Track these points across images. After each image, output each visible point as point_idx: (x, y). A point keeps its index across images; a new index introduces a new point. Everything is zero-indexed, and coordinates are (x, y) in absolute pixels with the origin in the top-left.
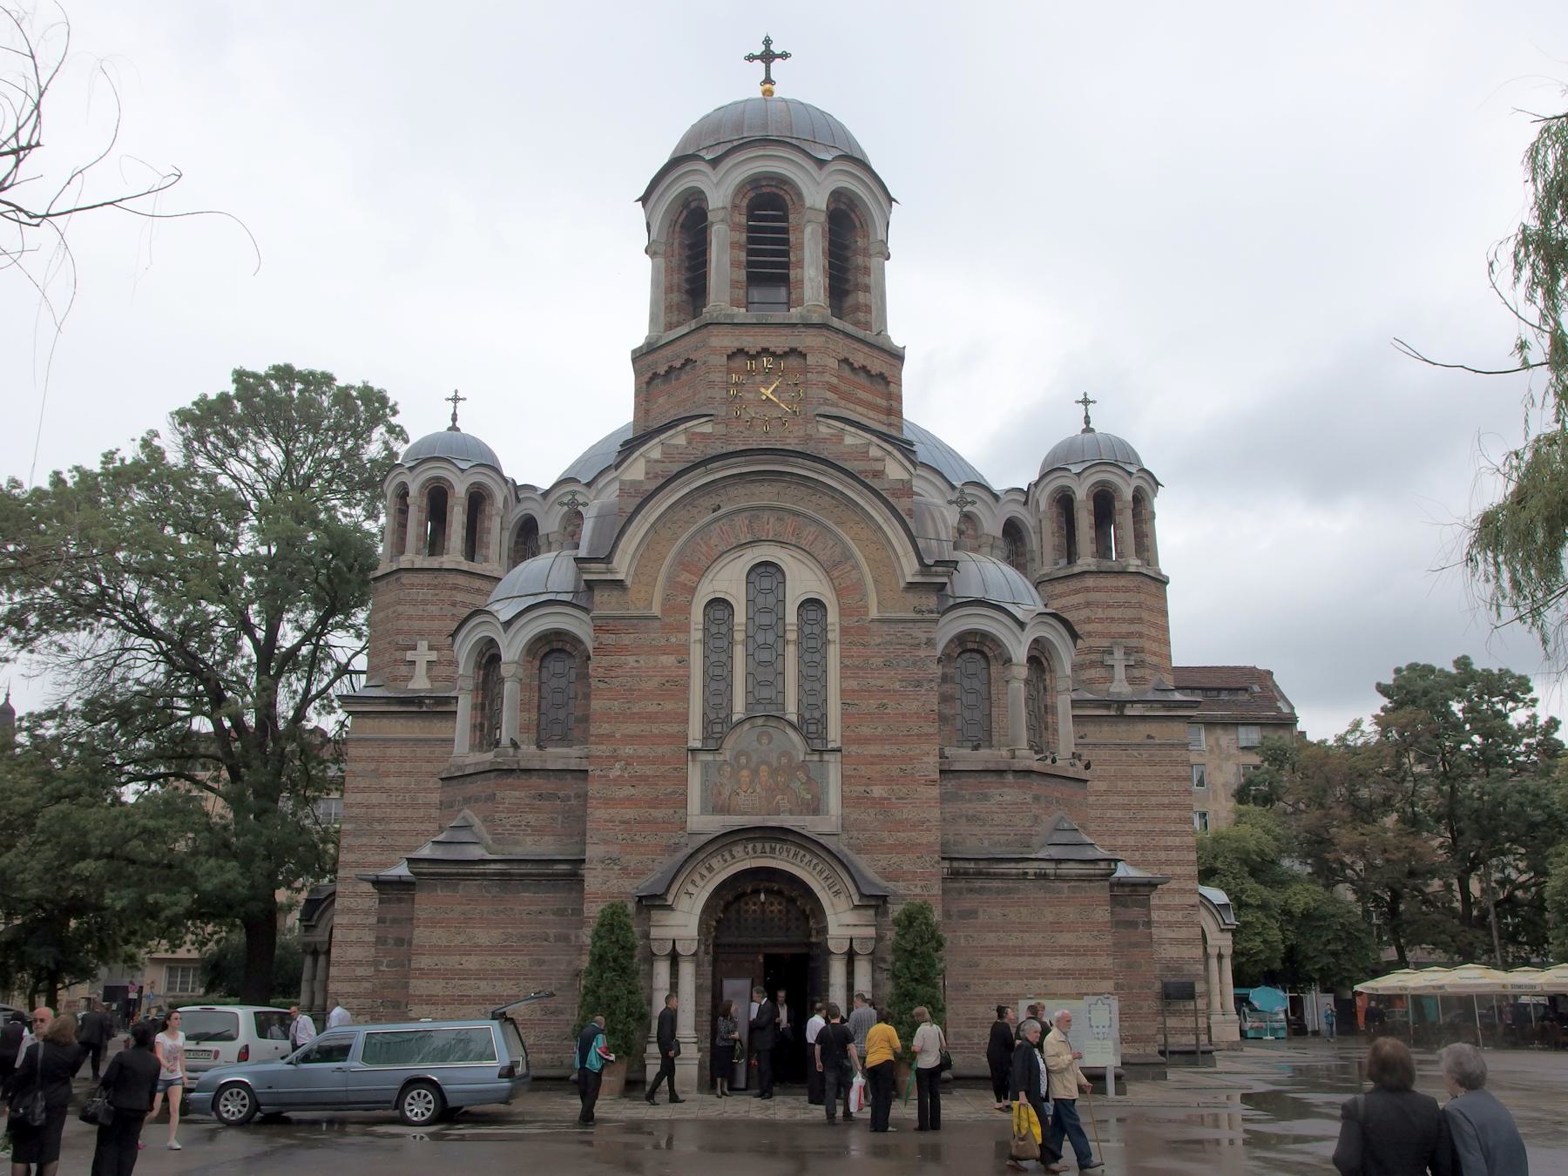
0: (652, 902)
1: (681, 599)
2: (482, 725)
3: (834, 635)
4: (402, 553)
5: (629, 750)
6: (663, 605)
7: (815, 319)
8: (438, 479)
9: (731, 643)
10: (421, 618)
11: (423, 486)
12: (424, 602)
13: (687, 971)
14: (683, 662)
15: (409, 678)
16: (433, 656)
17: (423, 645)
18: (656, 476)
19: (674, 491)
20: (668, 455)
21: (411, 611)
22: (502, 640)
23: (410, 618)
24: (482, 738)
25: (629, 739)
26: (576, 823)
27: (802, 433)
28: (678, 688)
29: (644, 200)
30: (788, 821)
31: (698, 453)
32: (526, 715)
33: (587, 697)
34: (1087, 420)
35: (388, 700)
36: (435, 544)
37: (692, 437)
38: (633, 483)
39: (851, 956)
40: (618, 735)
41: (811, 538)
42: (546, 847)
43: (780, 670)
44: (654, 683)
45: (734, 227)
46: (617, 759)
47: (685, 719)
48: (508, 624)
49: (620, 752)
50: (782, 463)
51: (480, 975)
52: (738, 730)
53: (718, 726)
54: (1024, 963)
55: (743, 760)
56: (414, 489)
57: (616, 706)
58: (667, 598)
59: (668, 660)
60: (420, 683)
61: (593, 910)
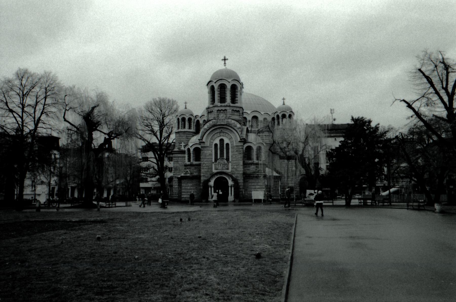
0: (209, 181)
3: (230, 147)
5: (205, 163)
7: (228, 105)
13: (213, 189)
17: (183, 143)
22: (190, 148)
25: (206, 161)
26: (200, 171)
28: (211, 155)
29: (207, 85)
30: (225, 171)
34: (284, 102)
39: (231, 187)
42: (195, 174)
45: (218, 91)
51: (190, 189)
53: (216, 159)
54: (254, 187)
59: (210, 151)
61: (202, 181)
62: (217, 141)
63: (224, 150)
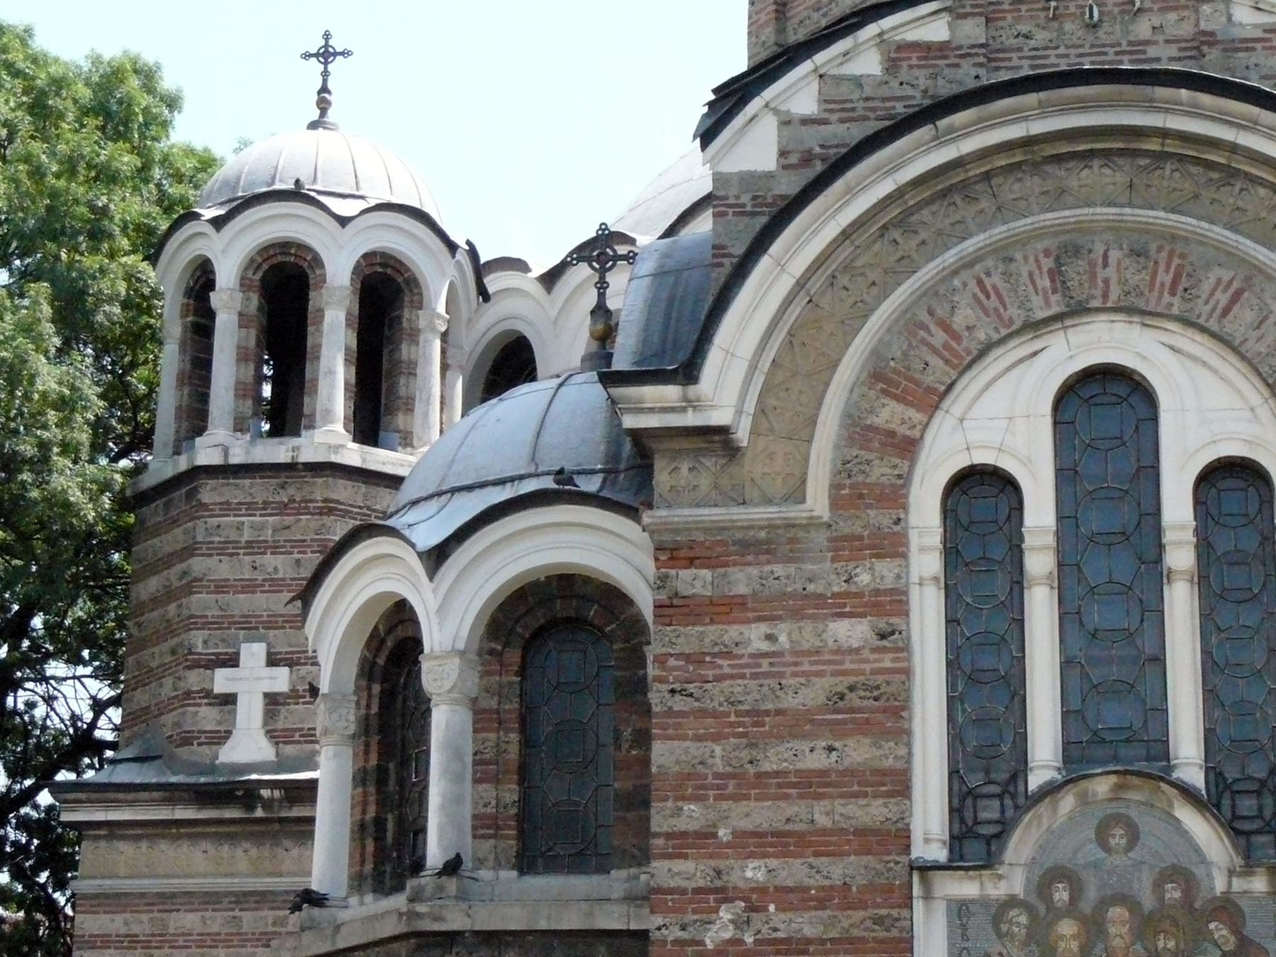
1: (880, 471)
2: (379, 822)
4: (200, 430)
5: (754, 872)
6: (835, 487)
8: (284, 246)
9: (1018, 584)
10: (250, 587)
11: (251, 264)
12: (254, 547)
14: (892, 637)
15: (221, 737)
16: (281, 680)
18: (807, 159)
19: (852, 193)
20: (836, 103)
21: (221, 568)
22: (424, 599)
23: (221, 587)
24: (381, 856)
25: (754, 842)
27: (1187, 29)
31: (920, 85)
32: (488, 791)
33: (643, 739)
35: (172, 794)
36: (286, 413)
37: (897, 55)
38: (749, 179)
40: (724, 833)
41: (1223, 298)
43: (1149, 650)
44: (813, 694)
46: (724, 895)
47: (898, 784)
48: (437, 557)
49: (734, 879)
50: (1128, 105)
52: (1043, 808)
53: (988, 800)
55: (1061, 894)
56: (227, 274)
57: (718, 755)
58: (843, 469)
59: (851, 632)
60: (247, 747)
62: (1005, 417)
63: (1154, 612)
